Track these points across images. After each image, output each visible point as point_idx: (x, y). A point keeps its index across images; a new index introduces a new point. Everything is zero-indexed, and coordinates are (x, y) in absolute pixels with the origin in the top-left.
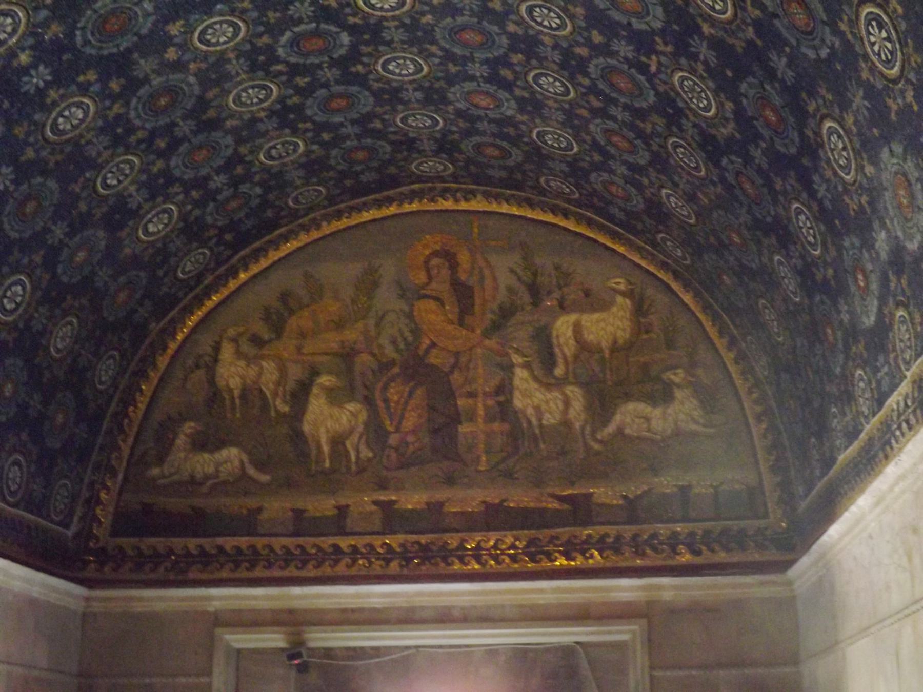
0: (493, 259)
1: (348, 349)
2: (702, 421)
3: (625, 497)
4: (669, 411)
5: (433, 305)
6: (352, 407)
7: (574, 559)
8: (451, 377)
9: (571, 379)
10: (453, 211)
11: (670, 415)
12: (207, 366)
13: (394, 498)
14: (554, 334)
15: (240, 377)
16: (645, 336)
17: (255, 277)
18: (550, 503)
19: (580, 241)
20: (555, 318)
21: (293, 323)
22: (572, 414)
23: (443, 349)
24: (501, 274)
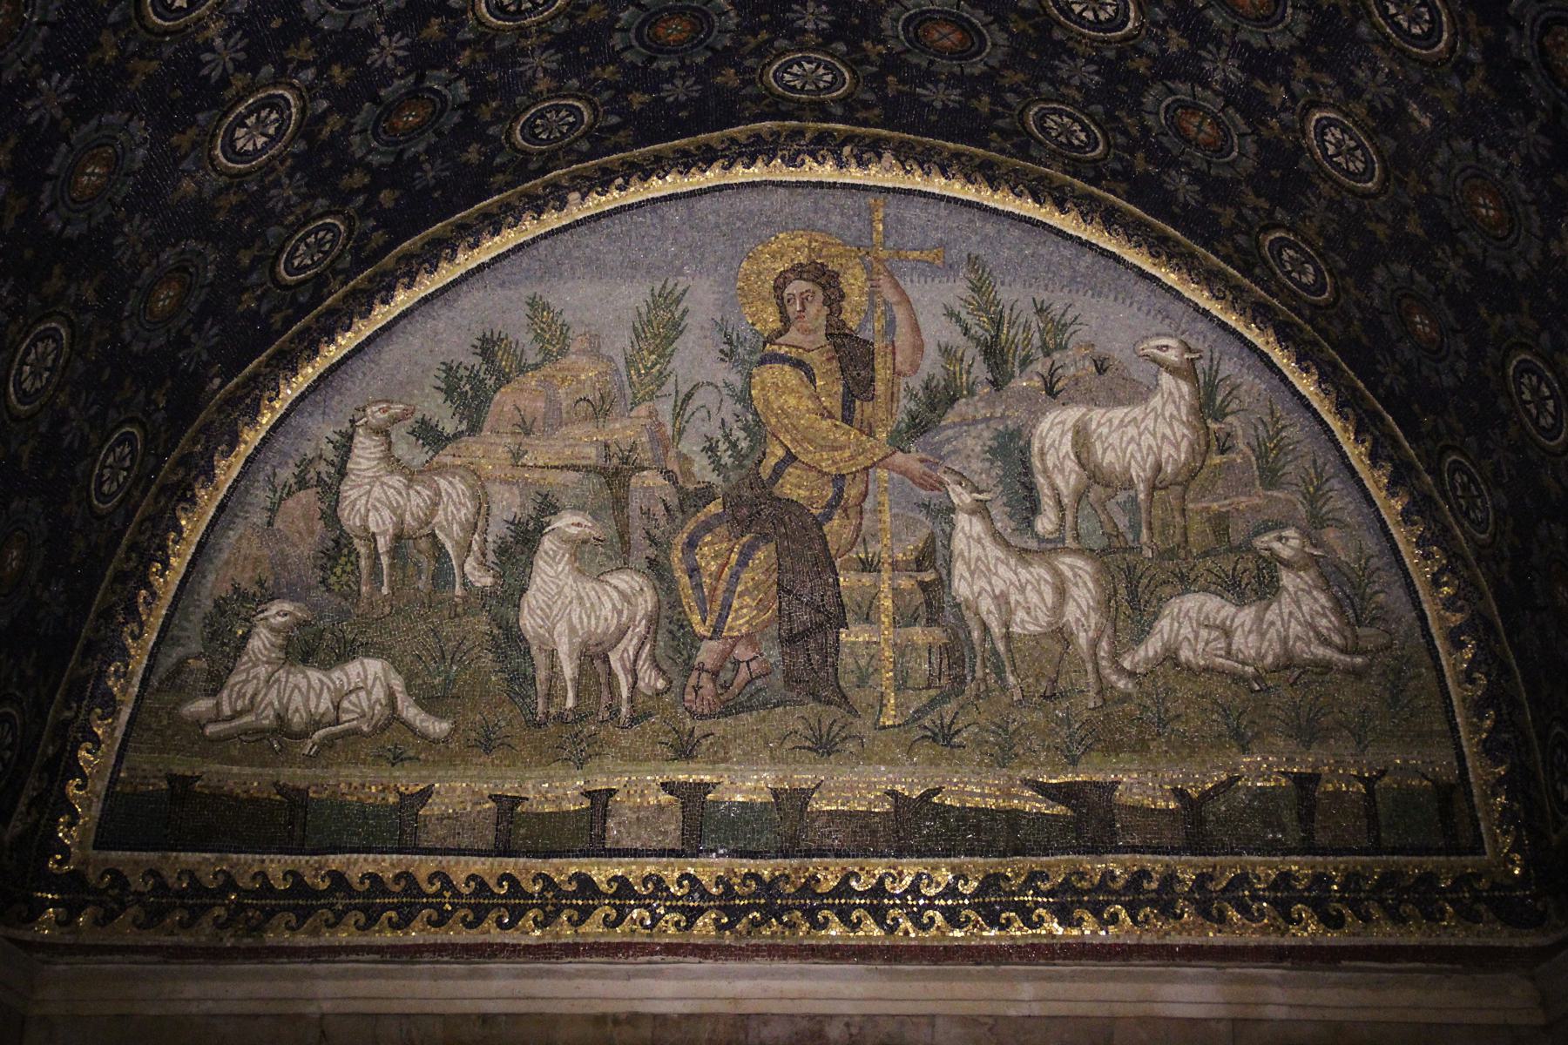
0: (913, 290)
1: (615, 461)
2: (1337, 639)
3: (1180, 794)
4: (1270, 616)
5: (790, 376)
6: (625, 581)
7: (1079, 923)
8: (826, 529)
9: (1069, 542)
10: (833, 185)
11: (1272, 623)
12: (320, 480)
13: (707, 778)
14: (1036, 446)
15: (394, 511)
16: (1217, 459)
17: (426, 300)
18: (1027, 799)
19: (1089, 257)
20: (1037, 415)
21: (505, 401)
22: (1071, 613)
23: (811, 468)
24: (928, 320)
